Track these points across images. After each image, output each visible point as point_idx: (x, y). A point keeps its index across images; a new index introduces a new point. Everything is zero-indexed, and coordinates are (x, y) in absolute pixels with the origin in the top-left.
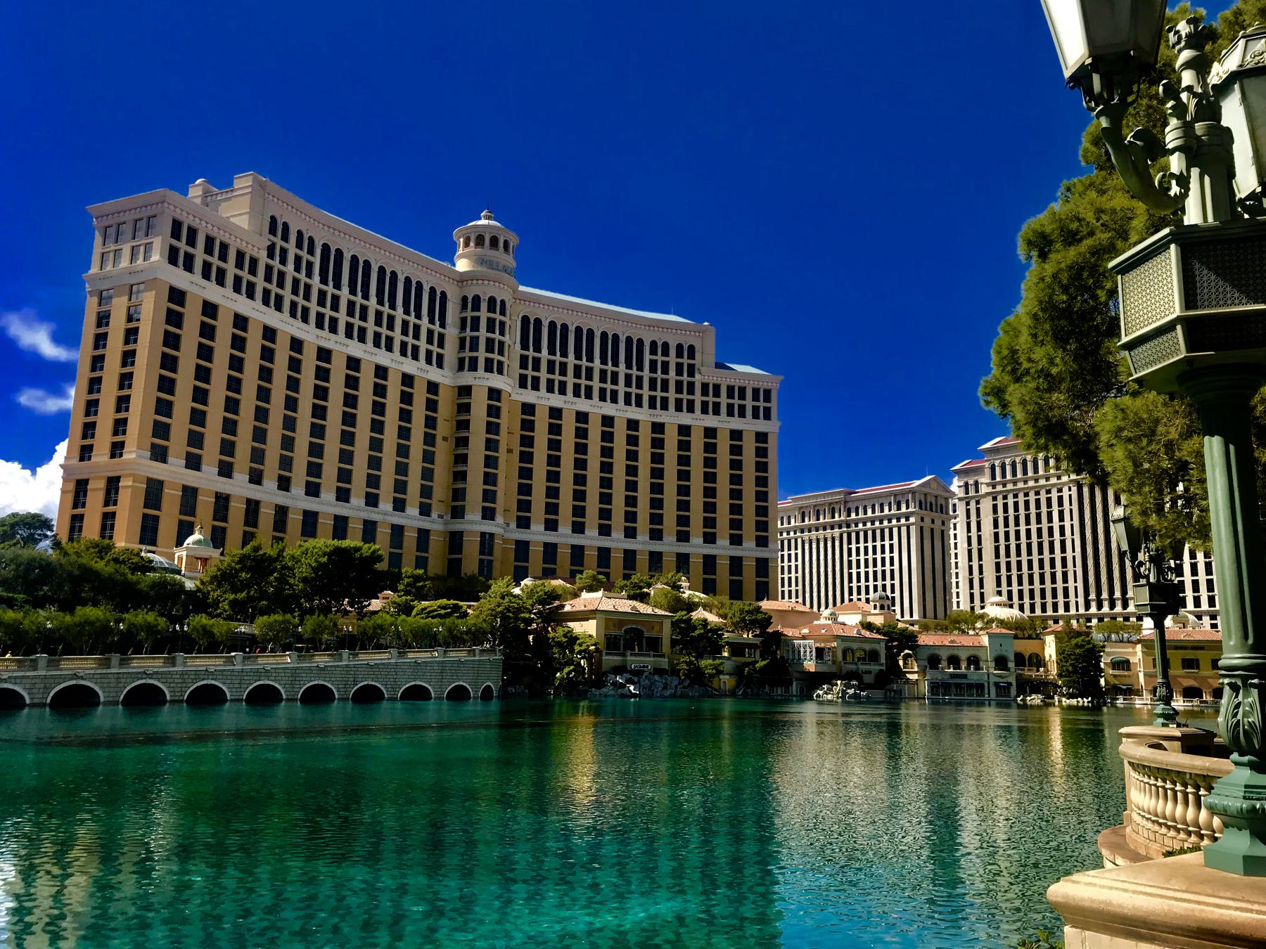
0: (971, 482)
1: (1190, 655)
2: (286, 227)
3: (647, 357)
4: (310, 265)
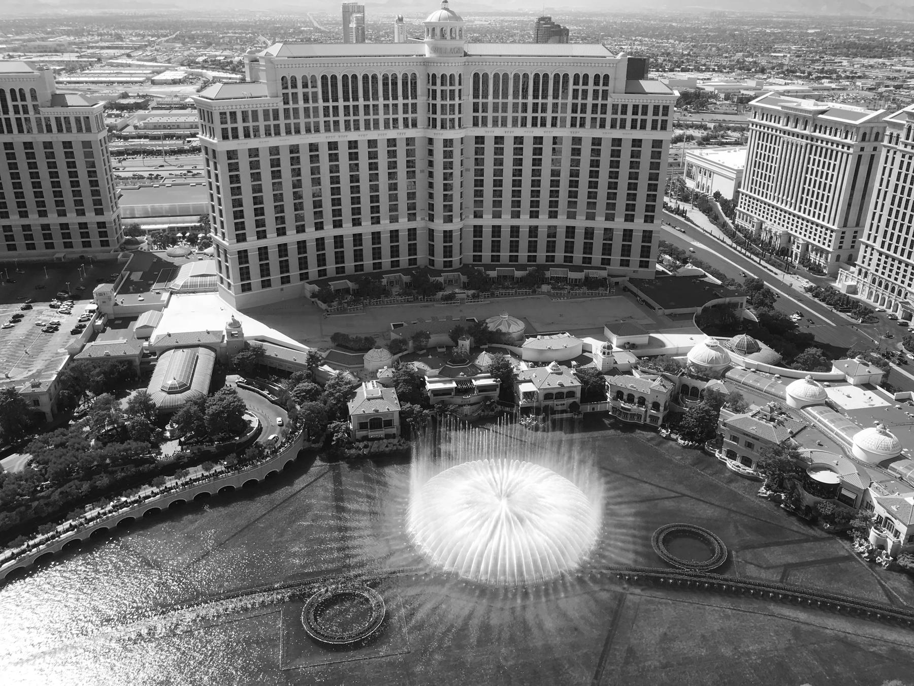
0: (895, 135)
1: (750, 440)
2: (294, 80)
3: (571, 87)
4: (315, 95)
